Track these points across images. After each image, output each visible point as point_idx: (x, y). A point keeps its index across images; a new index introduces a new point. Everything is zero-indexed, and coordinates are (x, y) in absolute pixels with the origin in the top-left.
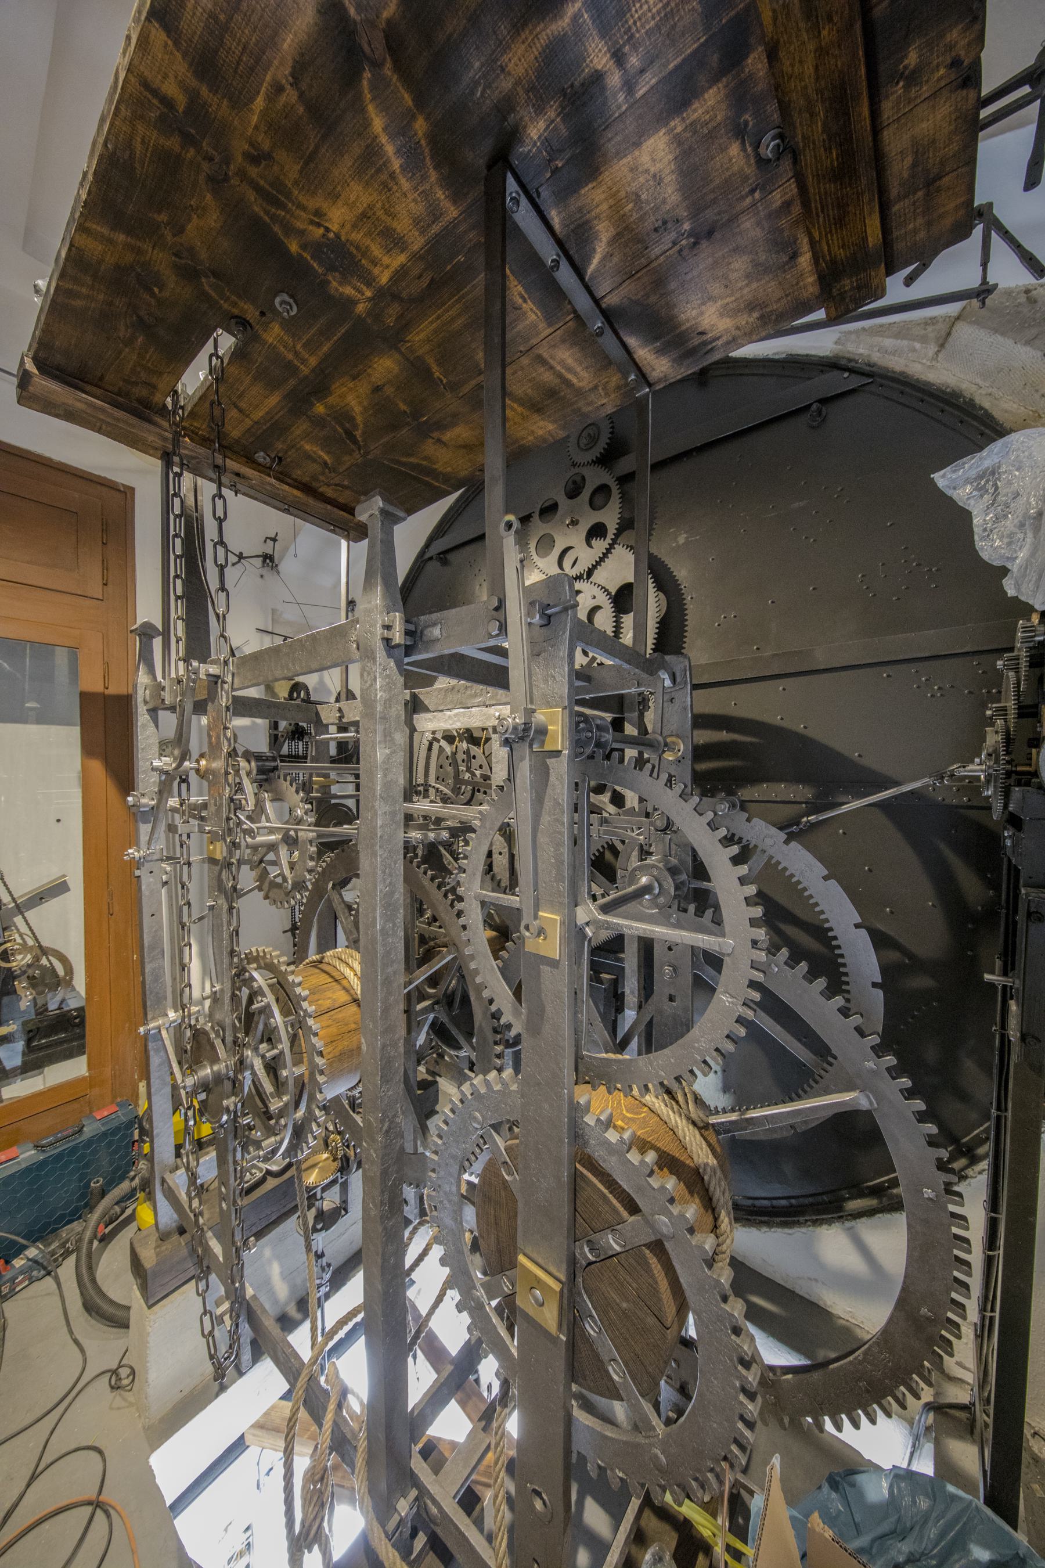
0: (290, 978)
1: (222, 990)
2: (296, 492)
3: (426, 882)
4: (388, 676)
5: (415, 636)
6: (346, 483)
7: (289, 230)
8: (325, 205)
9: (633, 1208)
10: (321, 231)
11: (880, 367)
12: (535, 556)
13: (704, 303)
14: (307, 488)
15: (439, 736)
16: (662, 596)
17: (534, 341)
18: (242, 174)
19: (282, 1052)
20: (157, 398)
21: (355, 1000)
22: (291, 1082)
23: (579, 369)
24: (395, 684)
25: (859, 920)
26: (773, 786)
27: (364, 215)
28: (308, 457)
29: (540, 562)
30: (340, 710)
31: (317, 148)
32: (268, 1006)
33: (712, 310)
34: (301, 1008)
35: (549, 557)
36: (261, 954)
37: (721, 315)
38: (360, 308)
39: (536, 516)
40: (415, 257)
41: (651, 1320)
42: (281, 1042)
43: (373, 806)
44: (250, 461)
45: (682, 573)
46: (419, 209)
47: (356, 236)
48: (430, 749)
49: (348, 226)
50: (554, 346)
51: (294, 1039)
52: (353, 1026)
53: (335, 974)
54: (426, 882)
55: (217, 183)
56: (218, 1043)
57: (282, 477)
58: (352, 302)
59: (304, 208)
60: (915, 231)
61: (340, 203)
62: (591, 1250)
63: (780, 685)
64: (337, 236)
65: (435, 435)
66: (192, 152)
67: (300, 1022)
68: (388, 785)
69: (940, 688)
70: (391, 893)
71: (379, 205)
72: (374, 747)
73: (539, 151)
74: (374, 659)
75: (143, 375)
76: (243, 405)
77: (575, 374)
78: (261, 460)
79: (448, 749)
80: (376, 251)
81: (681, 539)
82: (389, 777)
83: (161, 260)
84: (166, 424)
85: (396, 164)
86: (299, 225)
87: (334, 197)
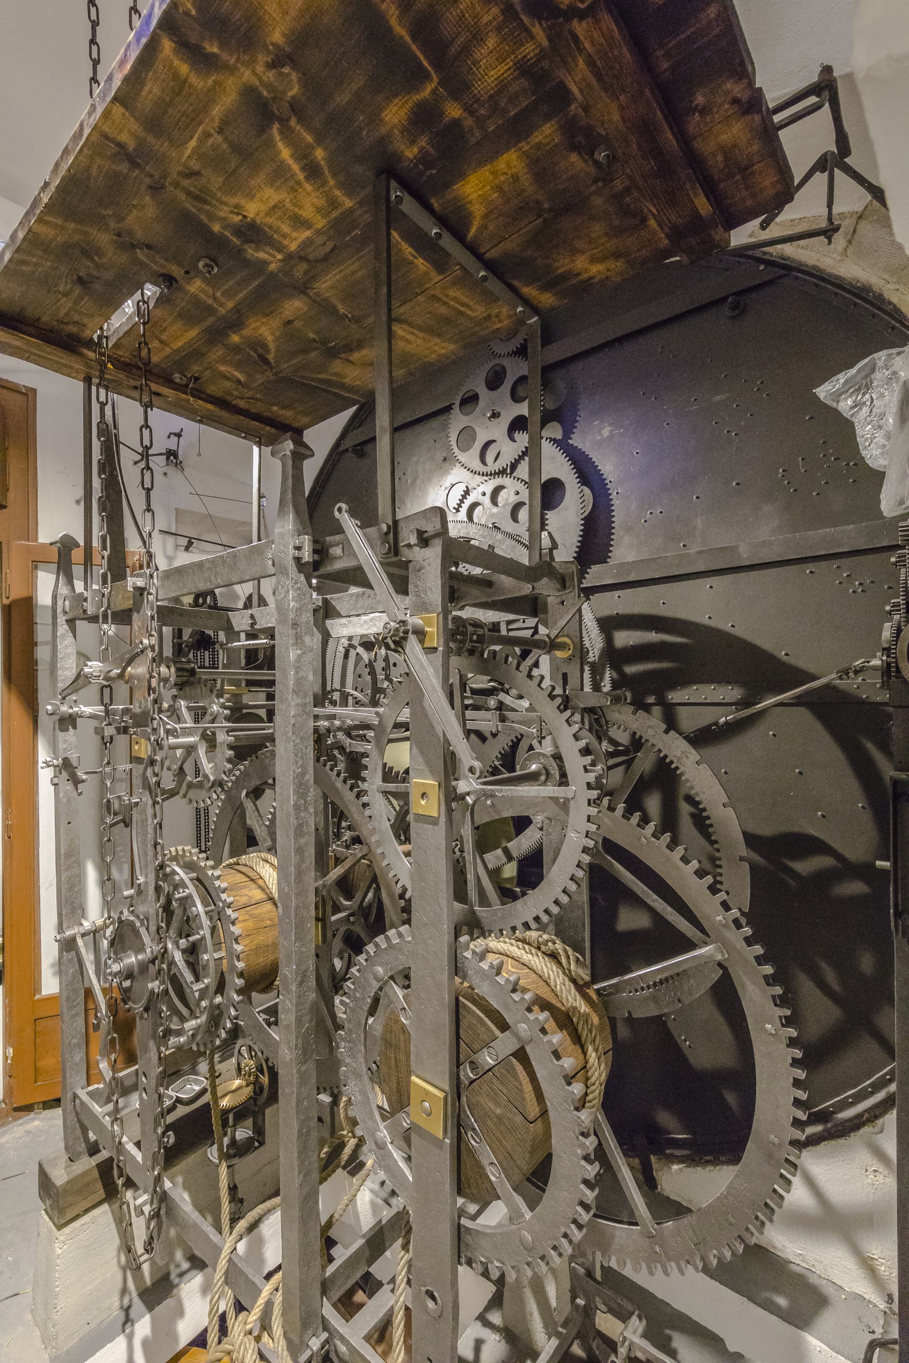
0: (210, 873)
1: (146, 883)
2: (211, 407)
3: (339, 784)
4: (299, 588)
5: (321, 552)
6: (258, 396)
7: (212, 217)
8: (243, 202)
9: (504, 1026)
10: (240, 217)
11: (793, 260)
12: (456, 450)
14: (221, 402)
15: (355, 642)
16: (587, 491)
17: (427, 285)
18: (176, 185)
19: (203, 938)
20: (87, 333)
21: (271, 899)
22: (212, 964)
23: (471, 304)
24: (305, 595)
25: (725, 799)
26: (702, 687)
28: (224, 377)
29: (462, 457)
30: (252, 617)
31: (237, 167)
32: (189, 897)
34: (221, 900)
35: (471, 451)
36: (181, 853)
38: (273, 267)
39: (456, 407)
40: (318, 232)
41: (519, 1118)
42: (203, 929)
43: (286, 699)
44: (168, 381)
45: (608, 466)
47: (270, 220)
48: (346, 656)
51: (213, 929)
52: (268, 923)
53: (251, 874)
54: (339, 784)
55: (156, 189)
56: (143, 931)
57: (198, 393)
58: (266, 263)
59: (226, 204)
62: (472, 1070)
63: (708, 582)
64: (253, 220)
65: (343, 355)
66: (137, 172)
67: (219, 913)
68: (299, 681)
69: (861, 584)
70: (304, 774)
72: (287, 649)
74: (287, 574)
75: (76, 318)
76: (164, 337)
77: (468, 306)
78: (177, 380)
79: (366, 656)
80: (286, 228)
81: (606, 432)
82: (301, 674)
83: (104, 239)
84: (91, 355)
85: (301, 176)
87: (251, 196)
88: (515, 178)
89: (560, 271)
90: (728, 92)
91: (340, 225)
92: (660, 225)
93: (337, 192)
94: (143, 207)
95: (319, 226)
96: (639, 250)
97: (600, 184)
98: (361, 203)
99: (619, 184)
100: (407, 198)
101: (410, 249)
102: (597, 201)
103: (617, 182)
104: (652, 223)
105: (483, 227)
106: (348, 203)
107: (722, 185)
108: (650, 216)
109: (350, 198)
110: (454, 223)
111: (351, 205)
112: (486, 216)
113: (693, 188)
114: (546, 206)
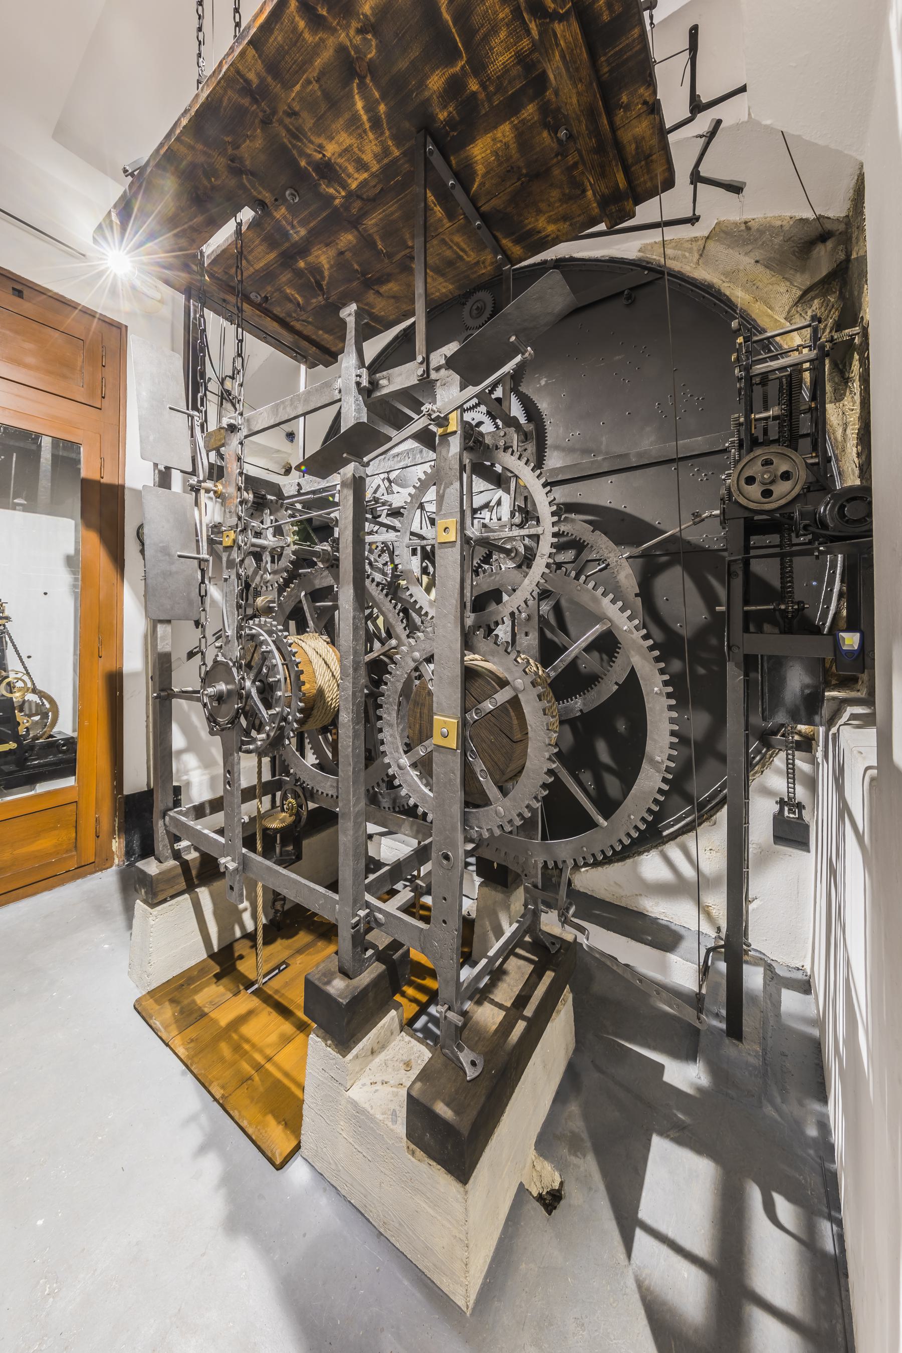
7: (302, 153)
8: (325, 143)
10: (321, 156)
13: (538, 215)
18: (281, 121)
27: (346, 150)
33: (543, 219)
37: (548, 222)
40: (373, 175)
46: (377, 149)
47: (339, 160)
49: (336, 155)
50: (453, 234)
55: (266, 122)
59: (312, 143)
60: (645, 182)
61: (333, 142)
64: (330, 159)
71: (356, 145)
73: (444, 126)
86: (309, 151)
87: (331, 138)
88: (507, 145)
89: (530, 226)
90: (641, 96)
91: (388, 171)
92: (594, 194)
93: (390, 143)
94: (254, 137)
95: (374, 170)
96: (580, 215)
97: (559, 158)
98: (404, 154)
99: (571, 160)
100: (436, 152)
101: (433, 198)
102: (556, 172)
103: (570, 158)
104: (590, 193)
105: (482, 184)
106: (396, 153)
107: (633, 169)
108: (589, 187)
109: (398, 148)
110: (464, 176)
111: (398, 154)
112: (484, 176)
113: (617, 165)
114: (524, 171)
